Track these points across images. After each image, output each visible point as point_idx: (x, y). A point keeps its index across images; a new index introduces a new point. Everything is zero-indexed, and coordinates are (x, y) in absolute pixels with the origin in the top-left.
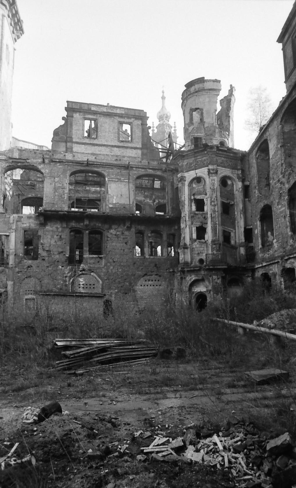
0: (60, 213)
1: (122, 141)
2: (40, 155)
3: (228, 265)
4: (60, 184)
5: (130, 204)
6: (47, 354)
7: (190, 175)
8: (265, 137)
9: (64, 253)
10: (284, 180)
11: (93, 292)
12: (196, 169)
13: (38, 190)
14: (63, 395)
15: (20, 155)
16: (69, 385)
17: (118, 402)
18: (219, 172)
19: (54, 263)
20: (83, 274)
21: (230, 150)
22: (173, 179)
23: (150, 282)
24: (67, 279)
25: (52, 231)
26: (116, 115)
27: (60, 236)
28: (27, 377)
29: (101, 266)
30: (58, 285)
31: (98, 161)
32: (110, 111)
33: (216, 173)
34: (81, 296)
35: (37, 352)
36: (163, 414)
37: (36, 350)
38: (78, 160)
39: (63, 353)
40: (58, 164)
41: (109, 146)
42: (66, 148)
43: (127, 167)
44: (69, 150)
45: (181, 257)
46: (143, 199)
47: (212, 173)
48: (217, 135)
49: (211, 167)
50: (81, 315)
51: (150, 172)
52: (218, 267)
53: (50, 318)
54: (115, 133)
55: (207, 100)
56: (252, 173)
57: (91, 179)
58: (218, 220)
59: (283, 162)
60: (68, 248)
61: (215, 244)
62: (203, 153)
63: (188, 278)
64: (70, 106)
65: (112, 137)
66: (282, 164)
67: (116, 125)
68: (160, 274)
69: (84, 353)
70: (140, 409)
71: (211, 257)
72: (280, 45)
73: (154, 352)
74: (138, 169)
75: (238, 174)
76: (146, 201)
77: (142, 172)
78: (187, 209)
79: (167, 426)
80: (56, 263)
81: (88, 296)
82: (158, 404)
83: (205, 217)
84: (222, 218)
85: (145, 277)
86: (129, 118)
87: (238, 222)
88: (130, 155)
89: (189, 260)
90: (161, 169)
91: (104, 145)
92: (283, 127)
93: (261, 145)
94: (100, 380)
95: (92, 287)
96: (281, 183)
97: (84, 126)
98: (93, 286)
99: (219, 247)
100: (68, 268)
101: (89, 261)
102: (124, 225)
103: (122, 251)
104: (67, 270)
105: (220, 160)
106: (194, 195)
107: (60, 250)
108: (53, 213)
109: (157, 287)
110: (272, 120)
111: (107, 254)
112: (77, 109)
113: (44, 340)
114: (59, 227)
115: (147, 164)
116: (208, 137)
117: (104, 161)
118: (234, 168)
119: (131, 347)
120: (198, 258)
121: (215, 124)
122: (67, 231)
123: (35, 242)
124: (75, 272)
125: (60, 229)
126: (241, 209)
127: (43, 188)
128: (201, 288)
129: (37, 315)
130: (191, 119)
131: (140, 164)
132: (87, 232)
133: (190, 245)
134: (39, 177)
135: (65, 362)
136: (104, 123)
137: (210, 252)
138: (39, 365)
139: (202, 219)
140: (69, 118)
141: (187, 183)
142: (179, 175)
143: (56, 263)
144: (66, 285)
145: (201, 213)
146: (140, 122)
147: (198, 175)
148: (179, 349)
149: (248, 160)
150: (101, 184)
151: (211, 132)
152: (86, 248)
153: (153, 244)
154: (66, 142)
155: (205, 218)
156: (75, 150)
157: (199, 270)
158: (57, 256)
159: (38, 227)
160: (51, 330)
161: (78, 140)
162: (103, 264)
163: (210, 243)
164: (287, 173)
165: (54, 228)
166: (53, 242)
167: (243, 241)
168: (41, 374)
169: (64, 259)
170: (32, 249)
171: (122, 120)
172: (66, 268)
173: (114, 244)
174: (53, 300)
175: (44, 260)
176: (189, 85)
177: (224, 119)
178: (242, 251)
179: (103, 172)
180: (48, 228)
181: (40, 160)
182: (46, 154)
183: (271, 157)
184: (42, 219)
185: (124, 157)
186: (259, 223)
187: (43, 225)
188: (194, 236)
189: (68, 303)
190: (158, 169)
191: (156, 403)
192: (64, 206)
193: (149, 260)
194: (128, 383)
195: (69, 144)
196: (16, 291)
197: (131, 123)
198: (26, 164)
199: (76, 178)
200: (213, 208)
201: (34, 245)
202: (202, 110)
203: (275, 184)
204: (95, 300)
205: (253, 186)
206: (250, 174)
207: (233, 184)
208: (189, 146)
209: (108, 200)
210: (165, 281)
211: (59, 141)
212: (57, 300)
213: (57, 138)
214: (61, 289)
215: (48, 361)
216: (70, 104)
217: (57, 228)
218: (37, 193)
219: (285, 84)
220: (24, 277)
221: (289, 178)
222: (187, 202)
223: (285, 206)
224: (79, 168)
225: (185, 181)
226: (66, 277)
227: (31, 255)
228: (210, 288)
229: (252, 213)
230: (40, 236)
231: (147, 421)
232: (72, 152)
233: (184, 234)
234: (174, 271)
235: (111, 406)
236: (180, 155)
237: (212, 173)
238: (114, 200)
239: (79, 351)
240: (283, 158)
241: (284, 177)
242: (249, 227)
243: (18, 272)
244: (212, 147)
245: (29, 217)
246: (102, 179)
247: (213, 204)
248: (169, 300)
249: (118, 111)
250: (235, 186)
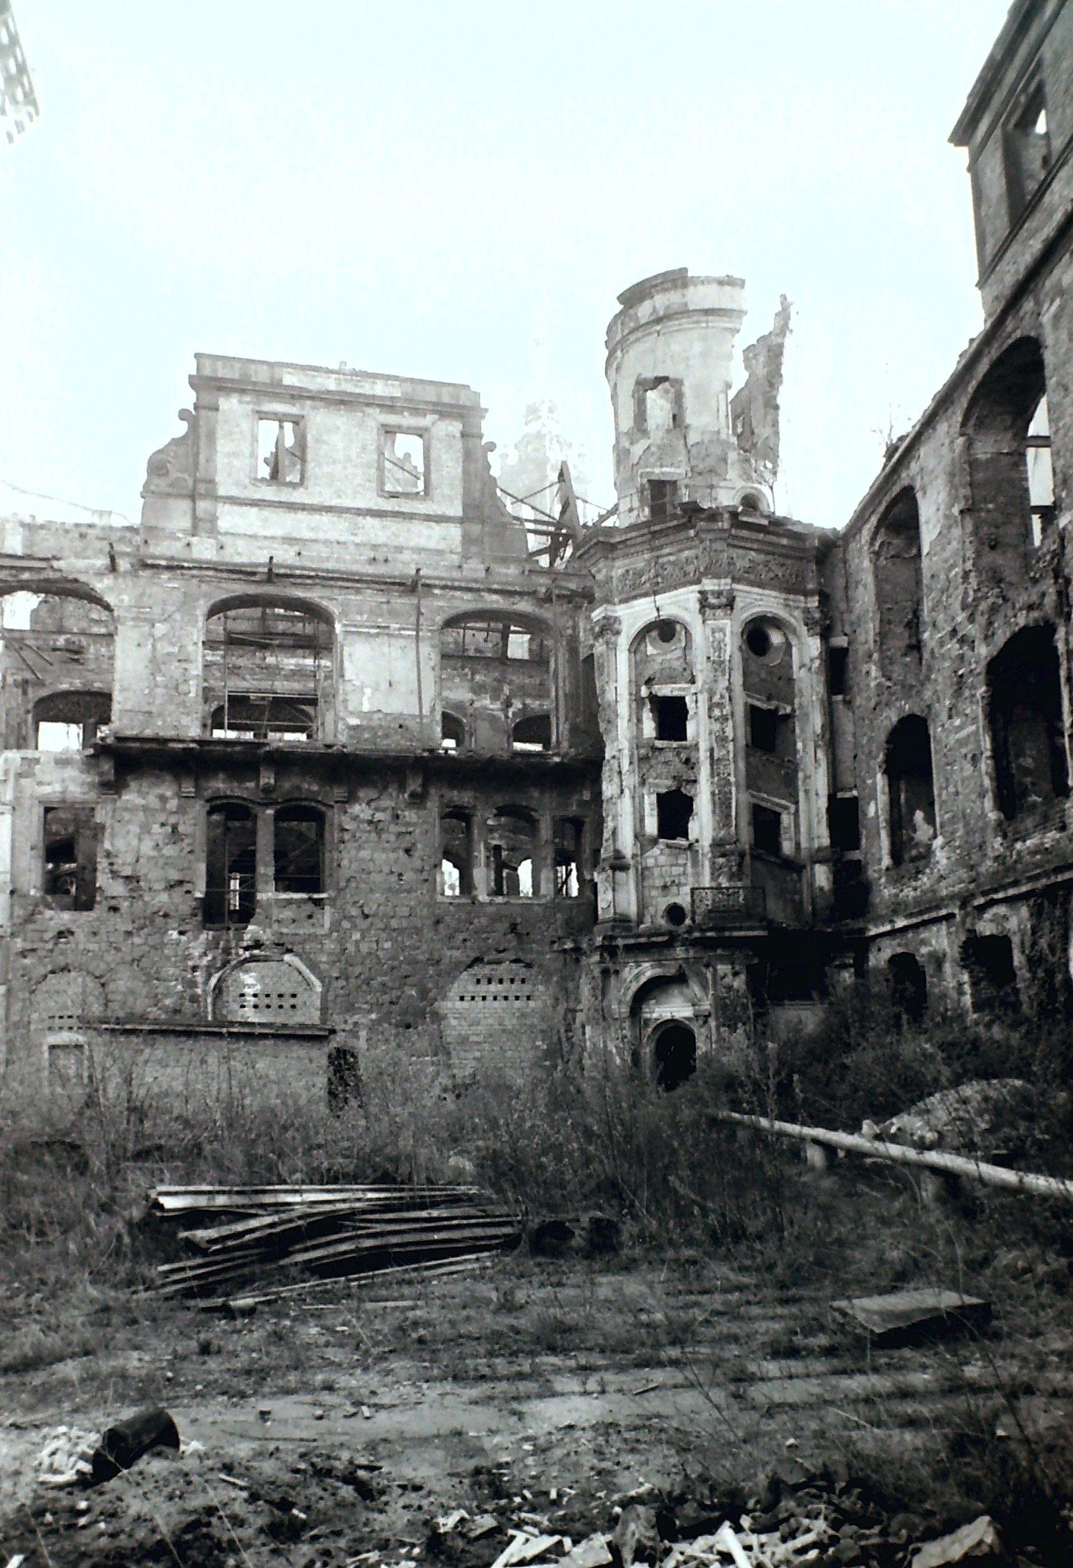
1: (394, 495)
2: (99, 544)
6: (127, 1240)
9: (187, 887)
11: (291, 1022)
15: (29, 543)
16: (205, 1349)
20: (254, 959)
26: (370, 402)
28: (53, 1321)
29: (320, 932)
30: (166, 996)
34: (250, 1035)
35: (89, 1232)
37: (88, 1227)
38: (237, 560)
39: (183, 1234)
40: (165, 576)
41: (347, 510)
42: (195, 517)
50: (247, 1101)
53: (138, 1112)
54: (368, 466)
57: (281, 626)
60: (202, 867)
64: (207, 372)
67: (371, 436)
69: (257, 1235)
80: (159, 921)
81: (274, 1036)
91: (329, 509)
97: (255, 439)
98: (293, 1001)
104: (198, 946)
107: (175, 876)
108: (147, 746)
111: (340, 890)
113: (115, 1189)
114: (169, 794)
117: (330, 565)
122: (198, 809)
123: (82, 846)
124: (227, 951)
125: (173, 804)
127: (112, 658)
129: (90, 1102)
134: (98, 622)
135: (192, 1268)
136: (329, 431)
138: (98, 1277)
140: (203, 413)
144: (194, 999)
150: (318, 644)
152: (266, 869)
154: (193, 497)
156: (223, 524)
158: (164, 897)
159: (92, 796)
160: (142, 1155)
161: (235, 492)
162: (327, 925)
166: (147, 848)
168: (106, 1309)
170: (71, 874)
171: (392, 419)
174: (147, 1051)
175: (115, 909)
184: (107, 766)
189: (203, 1062)
196: (15, 1018)
197: (426, 429)
198: (51, 575)
199: (231, 625)
201: (80, 858)
204: (298, 1051)
209: (345, 701)
212: (163, 1049)
213: (162, 484)
214: (176, 1011)
215: (128, 1265)
217: (163, 799)
220: (42, 971)
224: (239, 589)
226: (194, 969)
227: (68, 892)
239: (240, 1227)
243: (23, 954)
245: (62, 762)
246: (323, 627)
249: (380, 389)
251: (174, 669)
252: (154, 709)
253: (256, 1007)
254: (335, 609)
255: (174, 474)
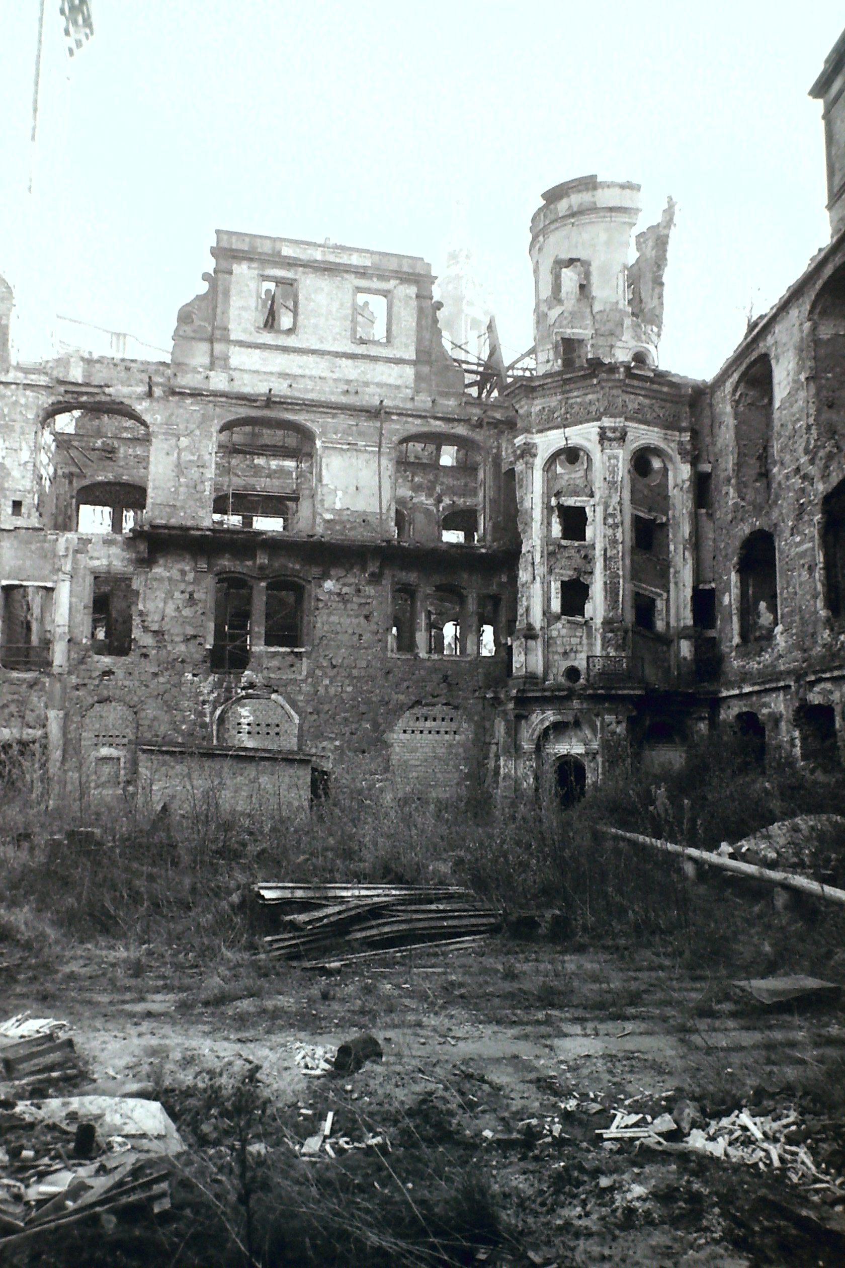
0: (192, 532)
1: (363, 342)
3: (646, 686)
4: (193, 455)
5: (381, 513)
7: (548, 442)
8: (762, 348)
9: (200, 640)
10: (812, 470)
12: (565, 427)
13: (122, 463)
14: (324, 1018)
15: (87, 374)
17: (458, 1039)
18: (630, 436)
19: (173, 667)
20: (248, 696)
21: (661, 377)
22: (499, 447)
23: (429, 724)
24: (208, 708)
25: (170, 579)
27: (191, 594)
31: (297, 394)
32: (332, 258)
33: (623, 438)
36: (574, 1069)
40: (189, 401)
41: (329, 353)
42: (212, 355)
43: (377, 413)
44: (216, 362)
45: (518, 660)
46: (410, 493)
47: (610, 440)
48: (627, 336)
49: (607, 422)
51: (438, 426)
52: (620, 692)
54: (345, 318)
55: (603, 237)
56: (720, 443)
58: (622, 568)
59: (811, 420)
60: (211, 626)
61: (612, 631)
62: (588, 382)
63: (536, 718)
65: (337, 330)
66: (809, 428)
68: (456, 702)
70: (516, 1057)
71: (598, 666)
72: (819, 105)
73: (492, 920)
74: (405, 419)
75: (680, 443)
76: (415, 500)
77: (415, 426)
78: (538, 531)
79: (592, 1095)
80: (178, 665)
82: (551, 1048)
83: (586, 557)
84: (632, 561)
85: (419, 711)
86: (382, 278)
87: (676, 572)
88: (385, 379)
89: (540, 670)
90: (467, 421)
91: (314, 352)
92: (814, 329)
93: (752, 369)
94: (389, 986)
95: (272, 733)
96: (805, 477)
98: (277, 730)
99: (624, 638)
100: (211, 678)
101: (266, 663)
102: (364, 569)
103: (356, 637)
104: (207, 686)
105: (633, 403)
106: (558, 494)
107: (190, 631)
108: (173, 532)
109: (447, 737)
110: (784, 307)
112: (243, 251)
114: (187, 568)
115: (430, 404)
116: (601, 341)
118: (670, 425)
119: (433, 907)
120: (564, 665)
121: (623, 305)
122: (209, 581)
124: (228, 690)
125: (190, 576)
126: (687, 536)
128: (570, 747)
130: (557, 286)
131: (409, 405)
132: (263, 584)
133: (542, 628)
137: (598, 650)
139: (578, 561)
140: (220, 276)
141: (539, 462)
142: (519, 440)
143: (178, 665)
144: (204, 725)
145: (576, 544)
146: (412, 290)
147: (571, 443)
148: (554, 917)
149: (711, 405)
151: (610, 326)
152: (258, 627)
153: (433, 617)
154: (211, 340)
155: (588, 559)
156: (234, 362)
157: (568, 698)
158: (182, 648)
159: (131, 569)
162: (304, 673)
163: (599, 625)
164: (821, 453)
165: (176, 574)
166: (170, 610)
167: (690, 622)
169: (198, 657)
171: (363, 283)
172: (206, 679)
173: (334, 619)
175: (145, 656)
176: (553, 196)
177: (645, 282)
178: (686, 648)
179: (309, 424)
180: (158, 570)
181: (142, 389)
182: (157, 372)
183: (777, 404)
184: (143, 547)
185: (366, 384)
186: (734, 577)
187: (146, 562)
188: (556, 606)
190: (459, 421)
191: (546, 1046)
192: (201, 513)
193: (428, 664)
194: (452, 996)
195: (219, 347)
198: (103, 398)
200: (610, 532)
202: (586, 264)
203: (787, 478)
205: (723, 475)
206: (714, 444)
207: (665, 470)
208: (548, 361)
209: (322, 501)
210: (470, 720)
211: (193, 338)
216: (225, 237)
217: (183, 573)
218: (121, 470)
219: (827, 213)
221: (827, 467)
222: (537, 514)
223: (812, 539)
224: (243, 412)
225: (535, 456)
228: (595, 746)
229: (716, 548)
230: (137, 593)
231: (543, 1084)
232: (226, 367)
233: (528, 598)
234: (496, 698)
235: (447, 1047)
236: (528, 387)
237: (610, 440)
238: (337, 500)
240: (812, 411)
241: (812, 462)
242: (707, 587)
244: (612, 369)
247: (610, 521)
248: (479, 773)
249: (355, 260)
250: (670, 474)
251: (194, 473)
252: (178, 504)
253: (249, 733)
254: (317, 430)
255: (197, 322)
